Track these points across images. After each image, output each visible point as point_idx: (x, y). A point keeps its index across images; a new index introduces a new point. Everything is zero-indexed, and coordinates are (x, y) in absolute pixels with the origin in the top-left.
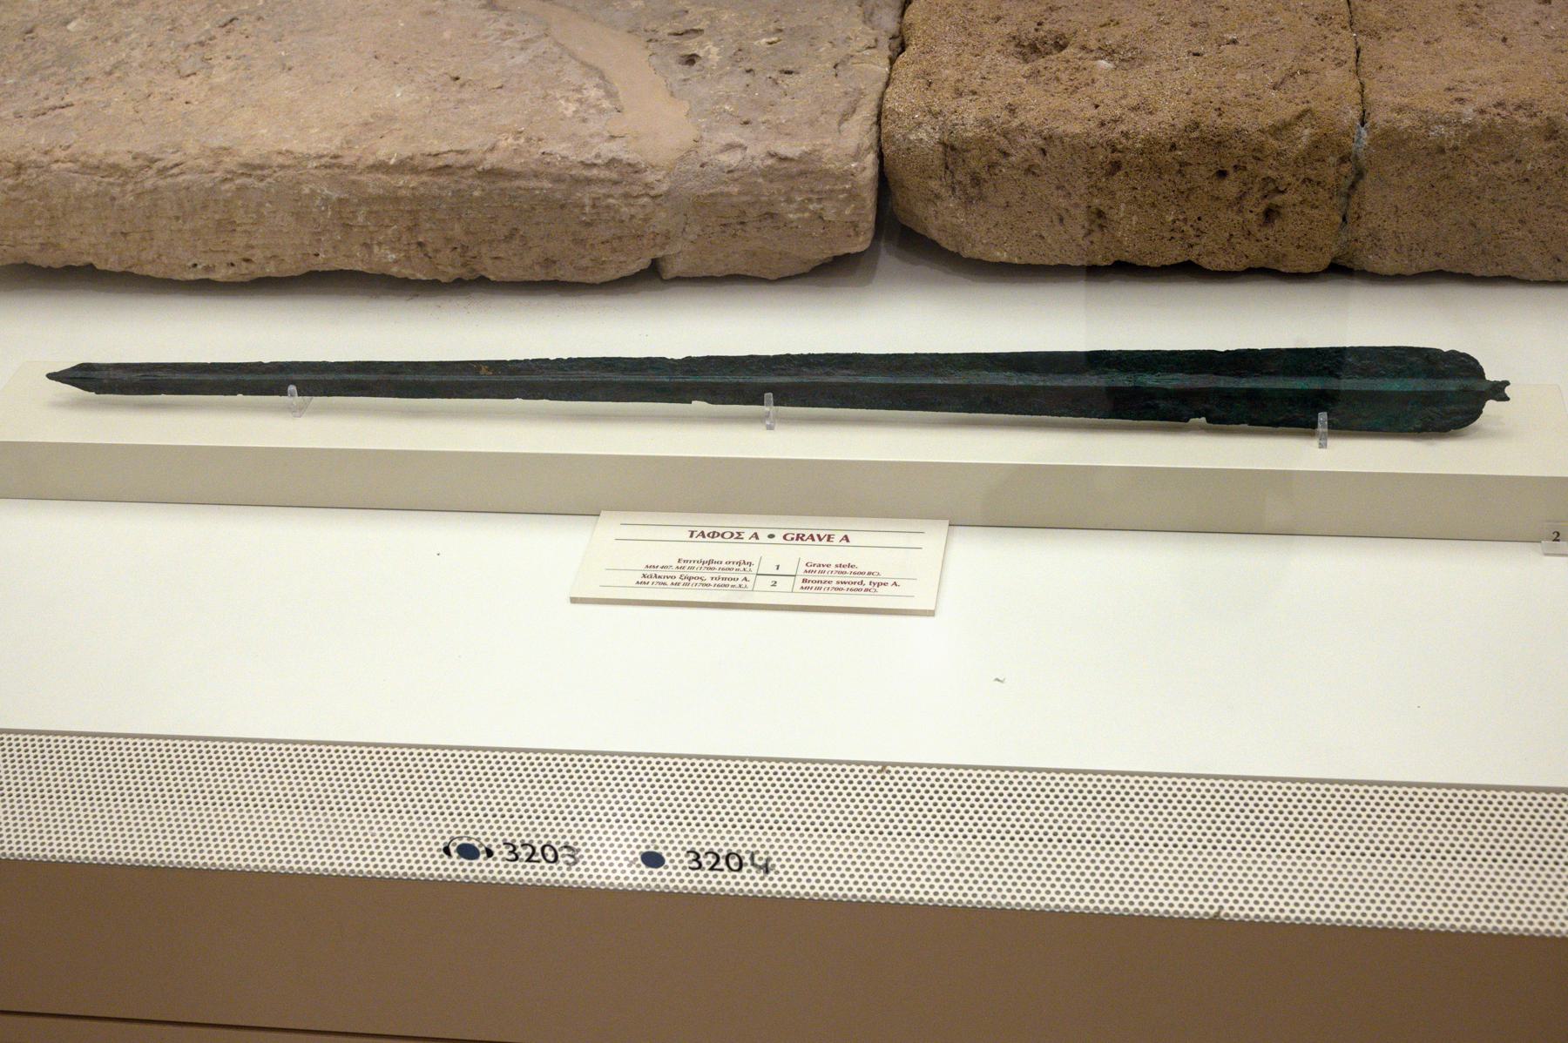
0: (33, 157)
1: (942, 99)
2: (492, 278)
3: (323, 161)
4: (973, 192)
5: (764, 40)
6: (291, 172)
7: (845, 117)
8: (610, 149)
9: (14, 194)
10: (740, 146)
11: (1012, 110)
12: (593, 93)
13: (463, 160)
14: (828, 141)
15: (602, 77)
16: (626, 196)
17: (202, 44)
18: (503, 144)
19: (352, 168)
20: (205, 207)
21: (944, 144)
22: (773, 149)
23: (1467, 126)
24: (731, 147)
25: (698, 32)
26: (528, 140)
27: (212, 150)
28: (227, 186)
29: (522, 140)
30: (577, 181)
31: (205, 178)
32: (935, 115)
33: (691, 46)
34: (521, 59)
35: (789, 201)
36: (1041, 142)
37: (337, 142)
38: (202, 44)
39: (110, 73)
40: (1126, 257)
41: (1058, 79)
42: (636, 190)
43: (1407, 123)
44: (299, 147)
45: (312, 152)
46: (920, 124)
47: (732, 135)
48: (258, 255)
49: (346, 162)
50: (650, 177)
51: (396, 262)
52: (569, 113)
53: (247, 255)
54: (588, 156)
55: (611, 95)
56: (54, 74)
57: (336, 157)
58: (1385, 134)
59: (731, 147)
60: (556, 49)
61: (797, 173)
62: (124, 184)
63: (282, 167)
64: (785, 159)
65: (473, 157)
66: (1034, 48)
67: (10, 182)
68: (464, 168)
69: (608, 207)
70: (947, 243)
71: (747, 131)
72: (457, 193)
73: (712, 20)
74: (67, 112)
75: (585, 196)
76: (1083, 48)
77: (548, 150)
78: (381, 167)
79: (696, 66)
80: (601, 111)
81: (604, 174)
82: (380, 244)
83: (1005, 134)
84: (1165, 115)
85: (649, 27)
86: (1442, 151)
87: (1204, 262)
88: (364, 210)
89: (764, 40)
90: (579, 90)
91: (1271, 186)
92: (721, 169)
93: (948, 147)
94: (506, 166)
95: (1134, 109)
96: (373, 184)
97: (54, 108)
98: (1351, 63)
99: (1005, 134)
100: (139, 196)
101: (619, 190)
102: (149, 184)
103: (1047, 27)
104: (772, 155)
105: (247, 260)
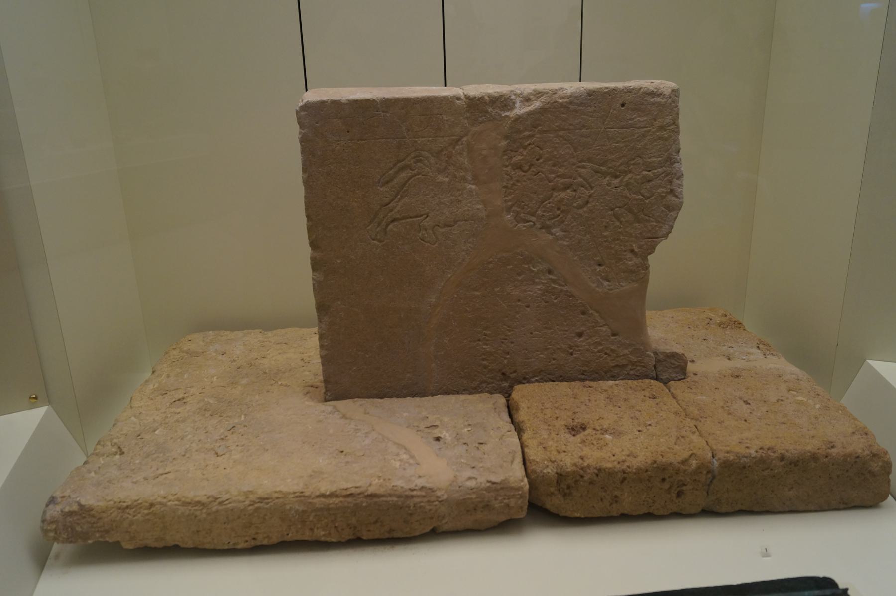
0: (159, 500)
1: (554, 455)
2: (364, 538)
4: (567, 491)
6: (281, 500)
7: (512, 462)
8: (421, 482)
11: (582, 458)
12: (405, 457)
13: (358, 491)
16: (428, 502)
17: (222, 439)
18: (374, 482)
19: (309, 497)
20: (239, 518)
21: (557, 473)
24: (470, 478)
28: (251, 508)
30: (408, 497)
32: (553, 462)
34: (367, 442)
35: (496, 500)
39: (184, 455)
40: (626, 512)
42: (433, 499)
43: (732, 458)
47: (469, 473)
48: (260, 537)
49: (307, 494)
50: (439, 493)
51: (324, 535)
53: (256, 536)
54: (412, 486)
55: (412, 457)
56: (158, 457)
58: (725, 462)
61: (500, 488)
63: (277, 498)
64: (494, 483)
66: (573, 429)
67: (146, 512)
68: (359, 494)
69: (421, 507)
70: (552, 510)
71: (475, 471)
72: (356, 505)
74: (170, 476)
75: (411, 503)
76: (594, 429)
78: (323, 496)
79: (441, 441)
80: (410, 464)
81: (419, 493)
84: (641, 458)
86: (744, 467)
87: (656, 513)
88: (313, 514)
90: (398, 455)
93: (560, 475)
94: (378, 492)
95: (628, 456)
96: (319, 503)
97: (162, 474)
99: (582, 469)
100: (209, 514)
102: (214, 509)
104: (488, 481)
105: (254, 539)
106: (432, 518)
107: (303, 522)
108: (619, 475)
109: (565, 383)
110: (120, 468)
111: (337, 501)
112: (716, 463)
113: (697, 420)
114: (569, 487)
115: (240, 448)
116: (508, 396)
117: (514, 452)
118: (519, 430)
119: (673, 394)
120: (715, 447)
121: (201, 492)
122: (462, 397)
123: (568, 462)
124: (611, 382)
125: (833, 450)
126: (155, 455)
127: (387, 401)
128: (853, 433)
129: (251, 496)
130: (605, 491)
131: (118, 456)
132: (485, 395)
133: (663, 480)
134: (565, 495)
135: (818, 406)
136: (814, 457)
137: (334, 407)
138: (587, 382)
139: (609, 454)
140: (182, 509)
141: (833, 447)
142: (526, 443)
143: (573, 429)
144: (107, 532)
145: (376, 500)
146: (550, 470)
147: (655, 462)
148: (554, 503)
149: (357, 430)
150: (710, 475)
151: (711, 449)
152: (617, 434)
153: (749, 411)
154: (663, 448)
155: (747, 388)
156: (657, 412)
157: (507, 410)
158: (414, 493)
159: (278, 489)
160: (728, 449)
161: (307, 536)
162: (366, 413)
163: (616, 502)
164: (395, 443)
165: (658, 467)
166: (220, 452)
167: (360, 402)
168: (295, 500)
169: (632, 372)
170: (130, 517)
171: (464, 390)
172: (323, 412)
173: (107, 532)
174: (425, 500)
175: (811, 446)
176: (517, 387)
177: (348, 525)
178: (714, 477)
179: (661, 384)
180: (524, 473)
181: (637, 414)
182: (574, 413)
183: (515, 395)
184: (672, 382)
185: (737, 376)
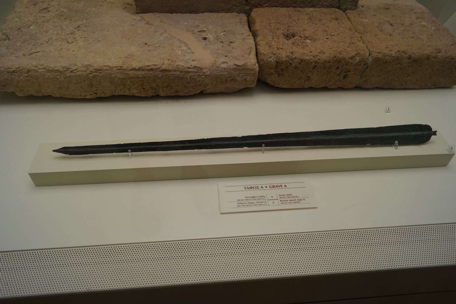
0: (32, 68)
3: (118, 68)
4: (281, 72)
5: (222, 34)
6: (109, 71)
7: (249, 54)
8: (194, 64)
9: (27, 78)
10: (226, 62)
12: (184, 48)
13: (156, 67)
14: (249, 61)
15: (185, 44)
16: (199, 75)
17: (72, 33)
19: (126, 70)
20: (84, 81)
21: (276, 61)
22: (235, 63)
23: (393, 57)
24: (224, 62)
25: (204, 31)
26: (172, 61)
27: (85, 65)
28: (91, 75)
29: (170, 62)
30: (186, 72)
31: (84, 73)
32: (274, 55)
33: (204, 35)
34: (162, 38)
35: (239, 76)
36: (300, 61)
37: (121, 62)
38: (72, 33)
39: (48, 42)
40: (313, 86)
41: (299, 45)
42: (201, 74)
43: (381, 56)
44: (111, 65)
45: (114, 66)
46: (271, 57)
47: (223, 59)
49: (124, 68)
50: (205, 71)
52: (180, 53)
53: (96, 92)
54: (189, 66)
55: (189, 49)
57: (121, 67)
58: (376, 59)
59: (224, 62)
60: (170, 36)
62: (61, 75)
63: (106, 70)
65: (158, 66)
66: (287, 36)
67: (26, 75)
68: (156, 69)
69: (194, 79)
70: (271, 83)
71: (227, 58)
73: (207, 28)
75: (188, 76)
76: (300, 36)
77: (178, 64)
78: (134, 69)
79: (207, 40)
80: (188, 53)
81: (193, 70)
82: (133, 89)
83: (291, 59)
85: (191, 30)
87: (329, 87)
88: (130, 80)
89: (222, 34)
90: (180, 47)
91: (348, 70)
92: (222, 68)
94: (168, 69)
95: (320, 53)
96: (132, 73)
97: (34, 53)
98: (362, 41)
100: (65, 78)
101: (197, 74)
102: (68, 75)
103: (290, 31)
105: (96, 93)
106: (200, 85)
107: (124, 85)
108: (313, 64)
109: (284, 9)
110: (7, 48)
111: (143, 73)
112: (370, 59)
113: (362, 33)
114: (282, 70)
115: (82, 39)
116: (248, 15)
117: (251, 48)
118: (255, 35)
119: (348, 18)
120: (371, 50)
121: (58, 63)
122: (221, 14)
123: (283, 55)
124: (312, 9)
125: (440, 54)
126: (29, 42)
127: (174, 15)
128: (452, 45)
129: (90, 68)
130: (303, 73)
131: (7, 41)
132: (235, 14)
133: (338, 68)
134: (279, 75)
135: (433, 28)
136: (428, 58)
137: (142, 17)
138: (298, 9)
139: (309, 51)
140: (48, 74)
141: (439, 52)
142: (258, 43)
143: (287, 36)
144: (5, 86)
145: (167, 73)
146: (272, 60)
147: (335, 57)
148: (272, 79)
149: (156, 32)
150: (365, 67)
151: (369, 50)
152: (314, 40)
153: (392, 30)
154: (341, 49)
155: (393, 16)
156: (338, 28)
157: (247, 24)
158: (190, 70)
159: (106, 64)
160: (379, 51)
161: (127, 93)
162: (161, 21)
163: (308, 80)
164: (179, 40)
165: (336, 60)
166: (70, 40)
167: (158, 15)
168: (117, 71)
169: (325, 4)
170: (17, 78)
171: (222, 10)
172: (135, 20)
173: (5, 86)
174: (197, 74)
175: (428, 51)
176: (255, 10)
177: (151, 87)
178: (367, 67)
179: (342, 12)
180: (256, 61)
181: (327, 28)
182: (289, 26)
183: (253, 14)
184: (348, 11)
185: (387, 9)
